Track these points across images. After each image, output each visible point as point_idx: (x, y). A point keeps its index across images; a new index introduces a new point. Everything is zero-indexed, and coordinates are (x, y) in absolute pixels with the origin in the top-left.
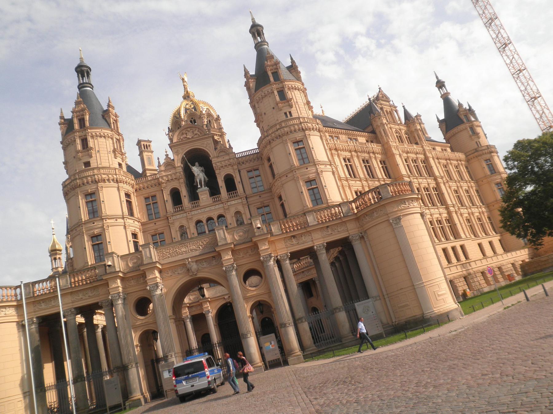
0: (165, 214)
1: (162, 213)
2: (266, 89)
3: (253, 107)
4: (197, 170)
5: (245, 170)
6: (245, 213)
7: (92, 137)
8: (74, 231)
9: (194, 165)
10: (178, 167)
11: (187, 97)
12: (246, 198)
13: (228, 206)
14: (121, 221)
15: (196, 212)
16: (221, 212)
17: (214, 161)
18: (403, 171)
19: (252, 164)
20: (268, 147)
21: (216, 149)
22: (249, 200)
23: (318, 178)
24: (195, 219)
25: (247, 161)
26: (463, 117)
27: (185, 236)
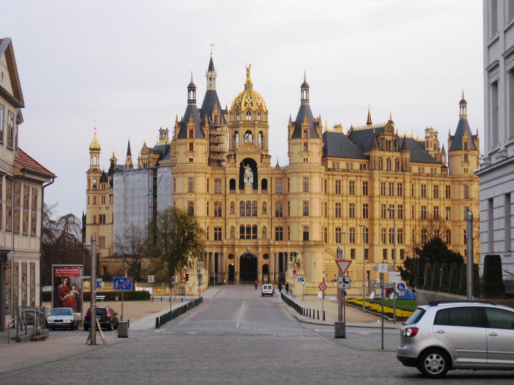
0: (225, 193)
1: (223, 192)
2: (298, 140)
3: (289, 144)
4: (248, 171)
5: (274, 178)
6: (268, 204)
7: (196, 144)
8: (179, 196)
9: (246, 166)
10: (238, 167)
11: (248, 86)
12: (271, 196)
13: (261, 197)
14: (204, 196)
15: (242, 196)
16: (256, 200)
17: (259, 169)
18: (377, 191)
19: (279, 176)
20: (290, 174)
21: (261, 161)
22: (272, 196)
23: (310, 201)
24: (241, 200)
25: (277, 174)
26: (463, 144)
27: (233, 209)
